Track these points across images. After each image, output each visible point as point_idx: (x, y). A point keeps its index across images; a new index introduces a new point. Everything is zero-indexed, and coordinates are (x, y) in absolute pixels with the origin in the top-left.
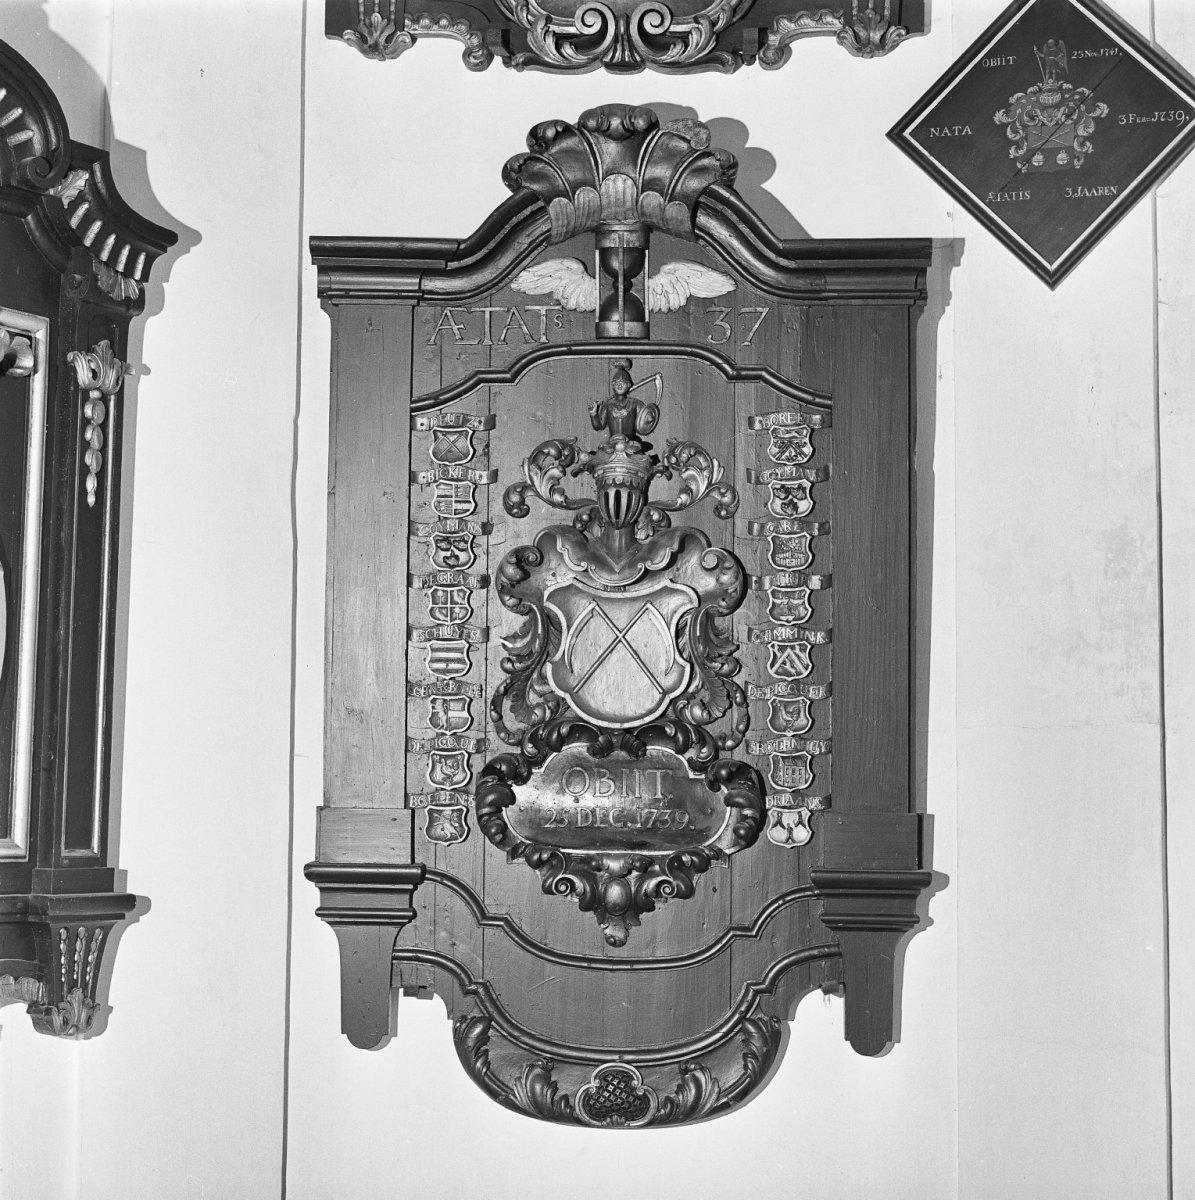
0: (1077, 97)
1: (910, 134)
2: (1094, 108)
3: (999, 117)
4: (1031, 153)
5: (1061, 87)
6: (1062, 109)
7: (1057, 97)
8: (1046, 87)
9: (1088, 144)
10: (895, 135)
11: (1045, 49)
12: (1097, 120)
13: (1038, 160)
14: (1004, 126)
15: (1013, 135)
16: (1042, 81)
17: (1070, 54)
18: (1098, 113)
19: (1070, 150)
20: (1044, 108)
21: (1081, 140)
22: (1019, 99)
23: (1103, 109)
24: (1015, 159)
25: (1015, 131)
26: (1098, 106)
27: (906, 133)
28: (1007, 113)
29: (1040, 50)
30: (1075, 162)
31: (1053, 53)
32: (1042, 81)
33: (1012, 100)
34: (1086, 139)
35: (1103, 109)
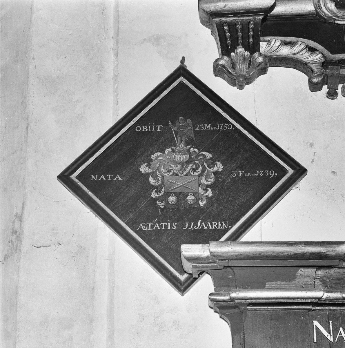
0: (201, 157)
1: (78, 177)
2: (214, 164)
3: (144, 169)
4: (168, 194)
5: (188, 150)
6: (190, 166)
7: (186, 157)
8: (177, 149)
9: (209, 189)
10: (64, 177)
11: (177, 123)
12: (216, 173)
13: (172, 199)
14: (147, 175)
15: (154, 181)
16: (175, 145)
17: (194, 127)
18: (215, 169)
19: (195, 194)
20: (177, 163)
21: (204, 187)
22: (158, 157)
23: (219, 167)
24: (156, 200)
25: (156, 178)
26: (216, 164)
27: (74, 176)
28: (149, 166)
29: (173, 123)
30: (200, 202)
31: (185, 126)
32: (175, 145)
33: (153, 157)
34: (208, 186)
35: (219, 167)
